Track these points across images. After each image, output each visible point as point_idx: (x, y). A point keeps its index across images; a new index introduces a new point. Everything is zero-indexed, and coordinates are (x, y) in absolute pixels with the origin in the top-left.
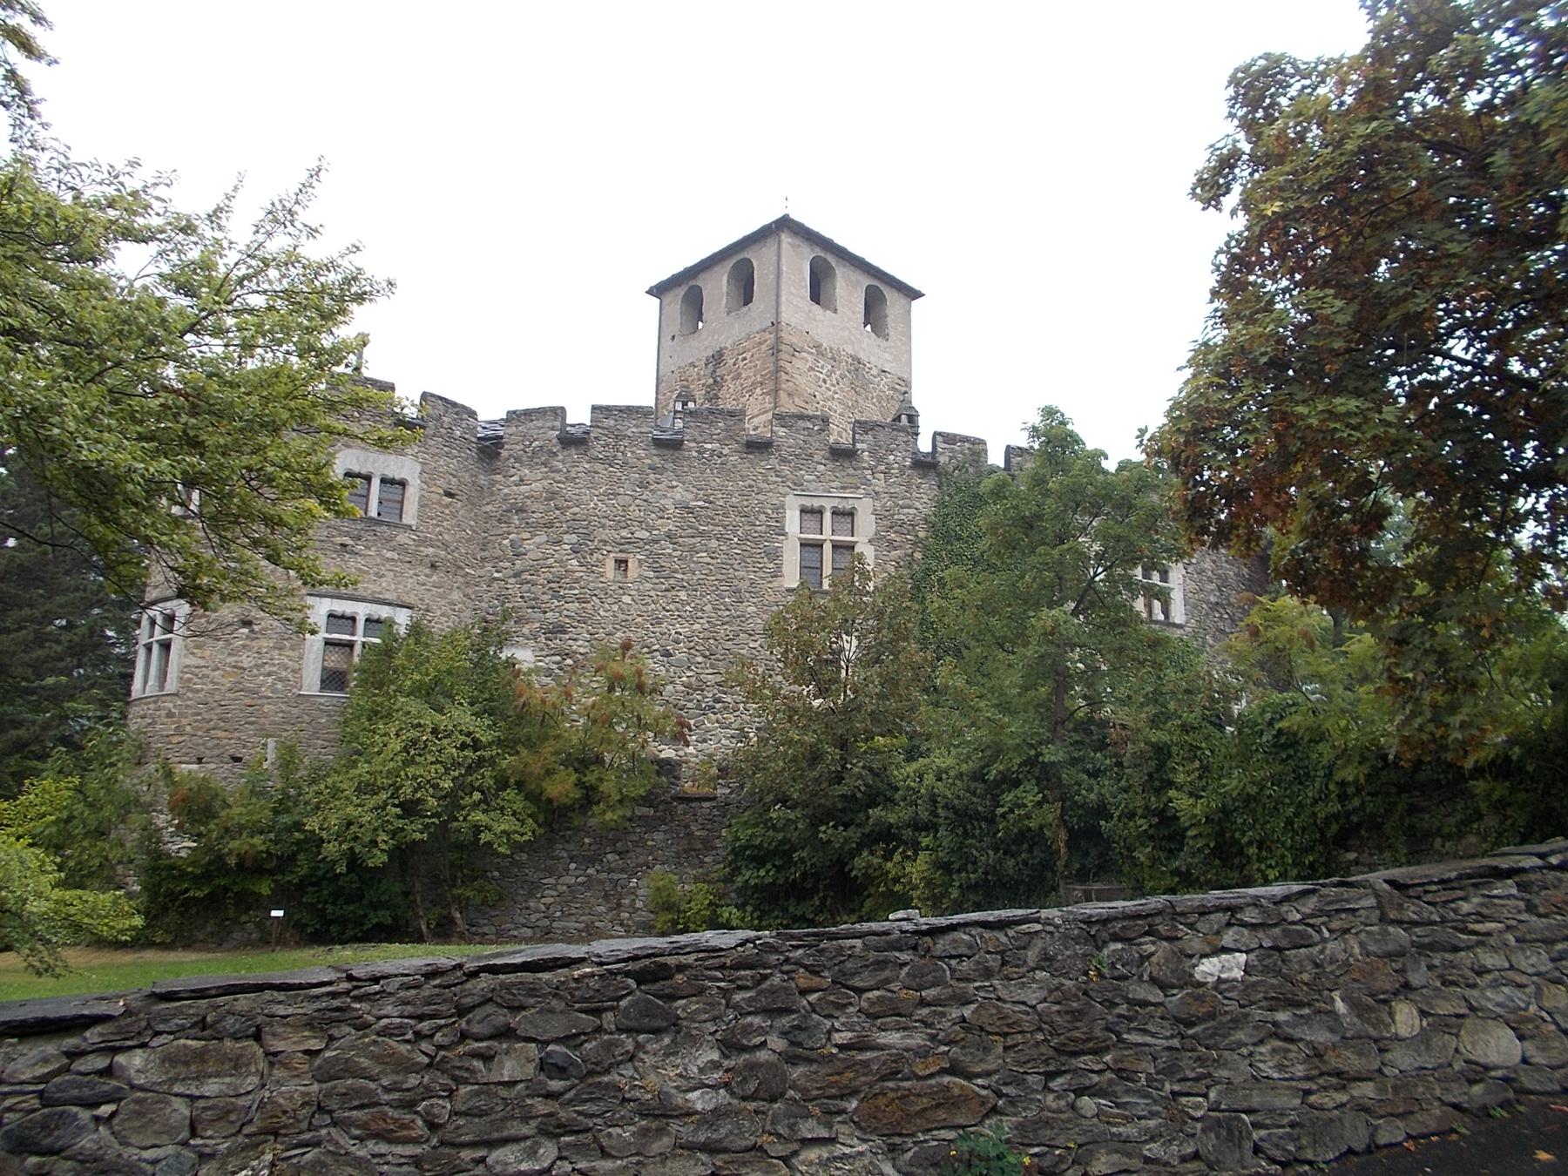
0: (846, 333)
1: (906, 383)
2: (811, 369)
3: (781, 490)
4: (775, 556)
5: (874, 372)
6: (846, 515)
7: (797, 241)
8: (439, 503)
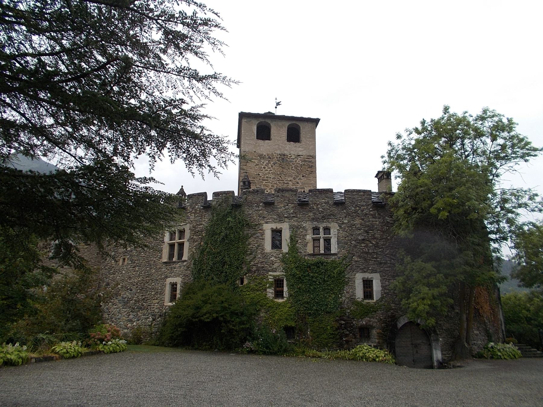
0: (277, 146)
1: (314, 157)
2: (257, 165)
4: (161, 251)
5: (293, 157)
6: (182, 233)
7: (249, 120)
8: (83, 248)
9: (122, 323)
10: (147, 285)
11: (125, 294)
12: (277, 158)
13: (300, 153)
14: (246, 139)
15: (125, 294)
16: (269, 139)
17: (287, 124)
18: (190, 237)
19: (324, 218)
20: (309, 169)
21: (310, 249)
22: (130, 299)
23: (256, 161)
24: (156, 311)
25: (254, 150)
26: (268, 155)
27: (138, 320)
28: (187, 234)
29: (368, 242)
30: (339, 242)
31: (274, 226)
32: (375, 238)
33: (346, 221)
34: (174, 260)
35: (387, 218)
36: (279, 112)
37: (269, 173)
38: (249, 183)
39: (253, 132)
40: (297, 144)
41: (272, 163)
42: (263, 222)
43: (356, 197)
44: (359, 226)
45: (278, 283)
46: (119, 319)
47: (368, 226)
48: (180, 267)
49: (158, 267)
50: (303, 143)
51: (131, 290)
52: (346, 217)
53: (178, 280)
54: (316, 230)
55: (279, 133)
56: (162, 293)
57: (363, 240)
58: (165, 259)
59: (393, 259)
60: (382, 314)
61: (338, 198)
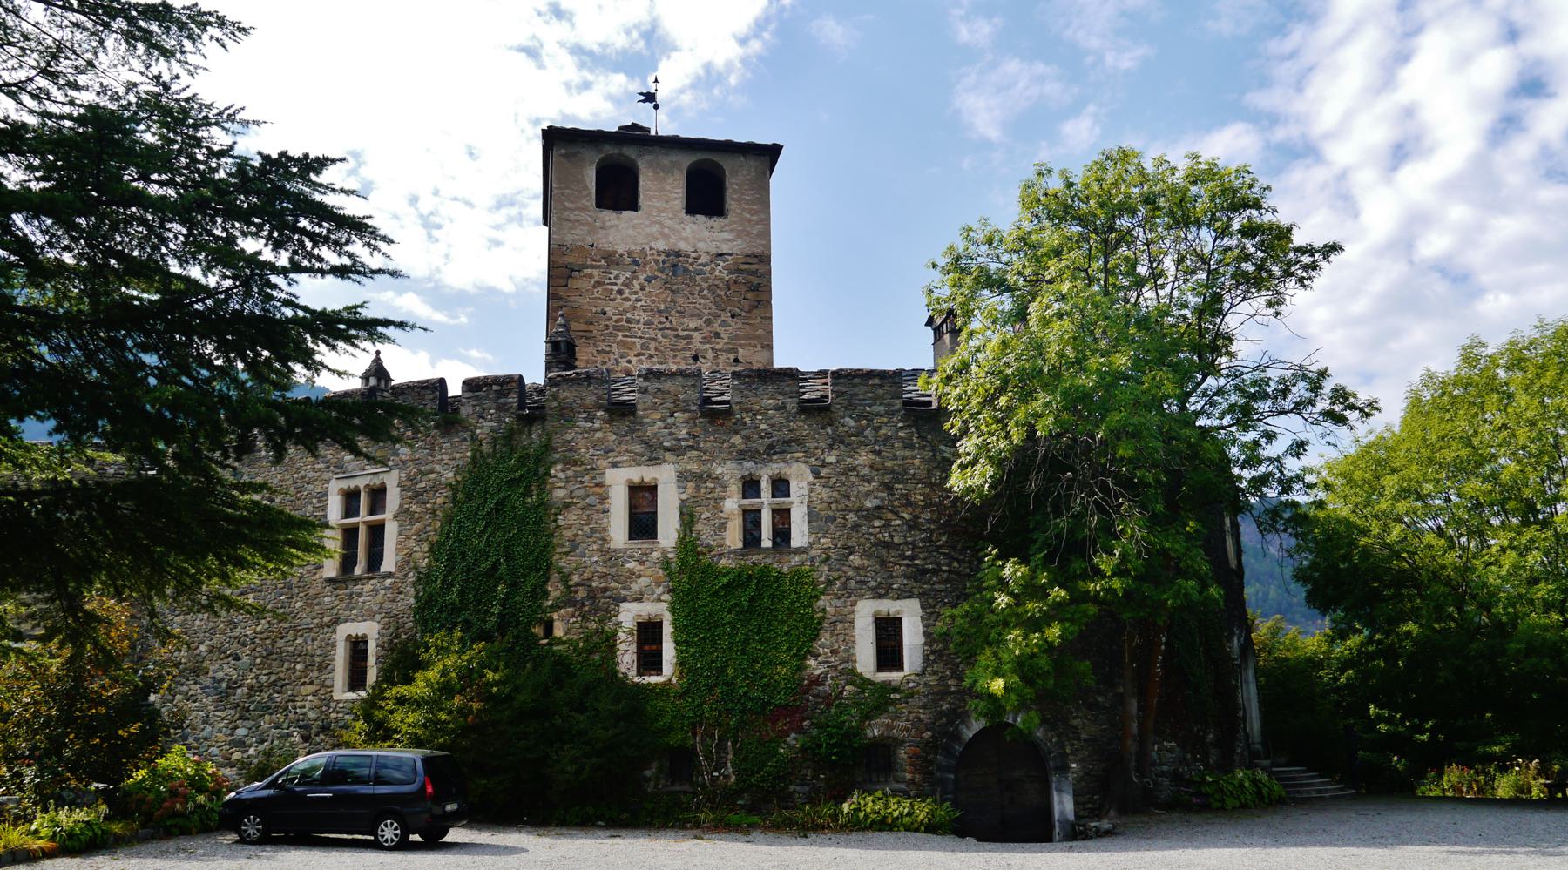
0: (656, 228)
1: (765, 259)
2: (598, 283)
3: (326, 476)
5: (704, 259)
6: (378, 496)
9: (215, 750)
10: (280, 643)
11: (221, 669)
12: (657, 261)
13: (725, 249)
14: (566, 209)
15: (221, 669)
16: (633, 206)
17: (687, 160)
18: (401, 506)
19: (771, 451)
20: (749, 296)
21: (733, 537)
22: (233, 686)
23: (596, 272)
24: (311, 715)
25: (589, 240)
26: (630, 253)
27: (262, 742)
28: (393, 499)
29: (890, 516)
30: (812, 516)
31: (636, 474)
32: (909, 504)
33: (832, 459)
34: (358, 571)
35: (942, 447)
36: (662, 124)
37: (635, 308)
38: (571, 347)
39: (586, 187)
40: (716, 222)
41: (642, 277)
42: (602, 463)
43: (860, 390)
44: (866, 471)
45: (649, 632)
46: (206, 739)
47: (893, 472)
48: (375, 592)
49: (312, 592)
50: (732, 217)
51: (237, 658)
52: (831, 447)
53: (370, 629)
54: (750, 487)
55: (662, 191)
56: (325, 666)
57: (878, 508)
58: (331, 569)
59: (959, 561)
60: (924, 707)
61: (813, 390)
